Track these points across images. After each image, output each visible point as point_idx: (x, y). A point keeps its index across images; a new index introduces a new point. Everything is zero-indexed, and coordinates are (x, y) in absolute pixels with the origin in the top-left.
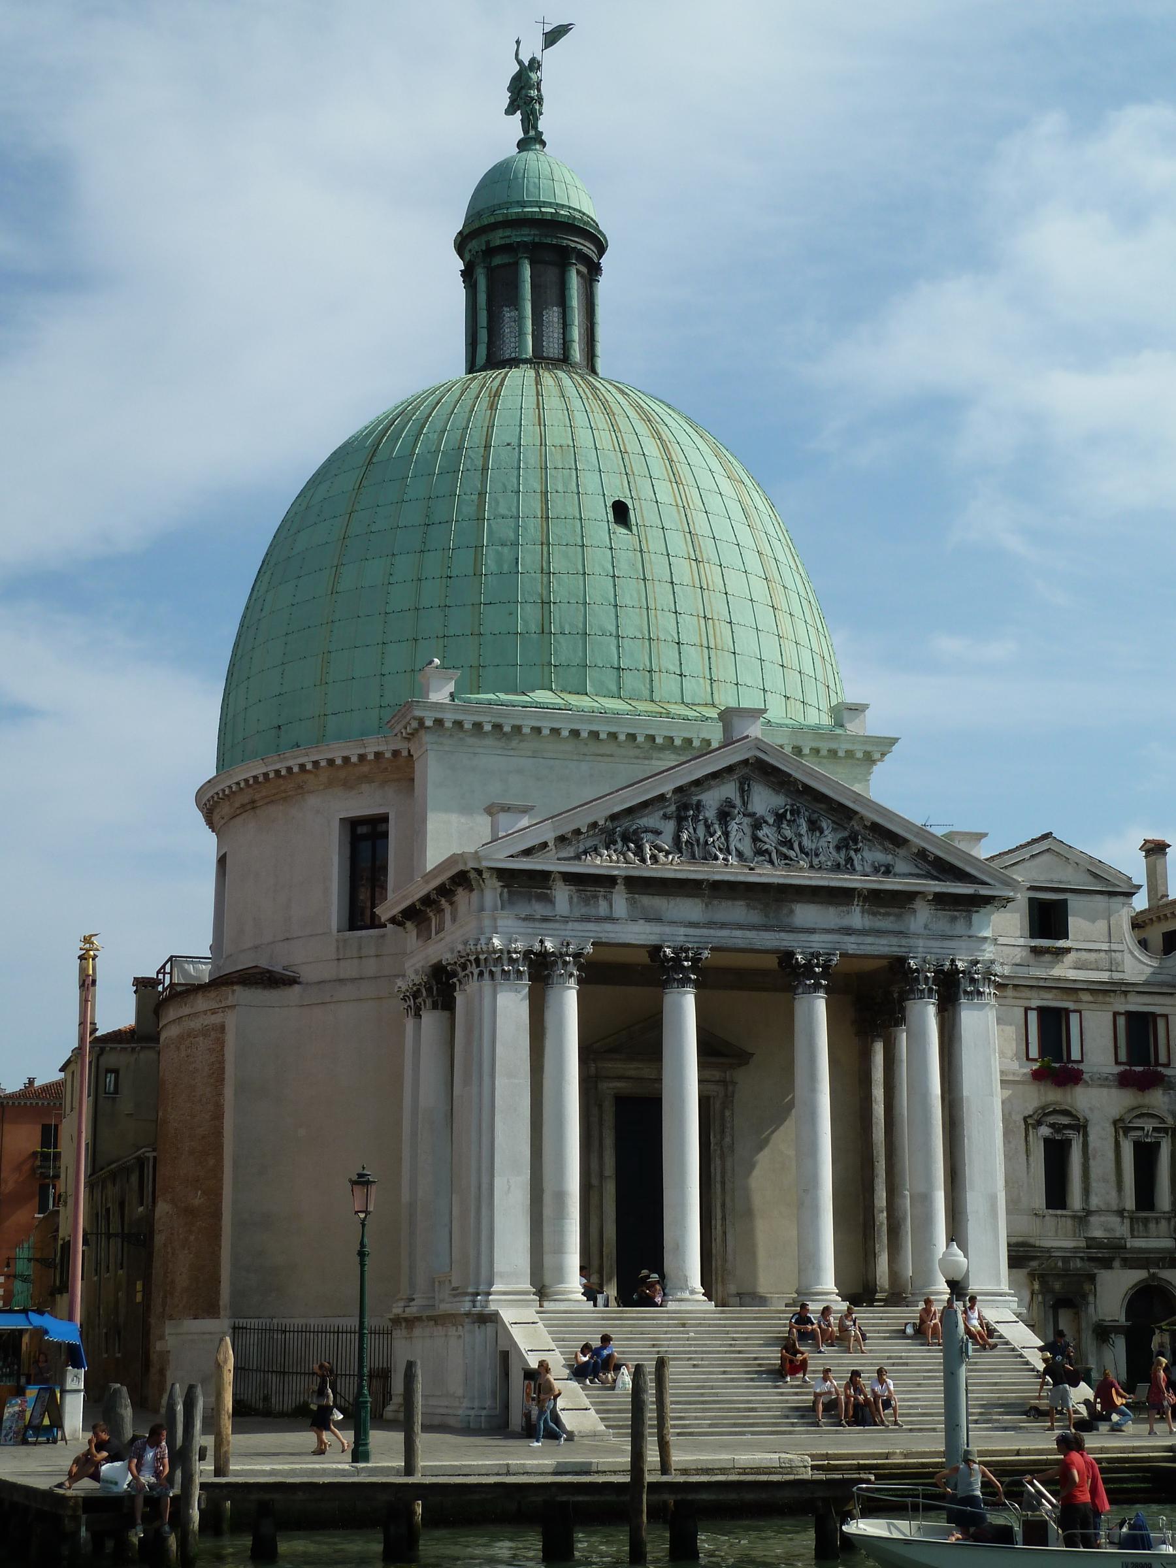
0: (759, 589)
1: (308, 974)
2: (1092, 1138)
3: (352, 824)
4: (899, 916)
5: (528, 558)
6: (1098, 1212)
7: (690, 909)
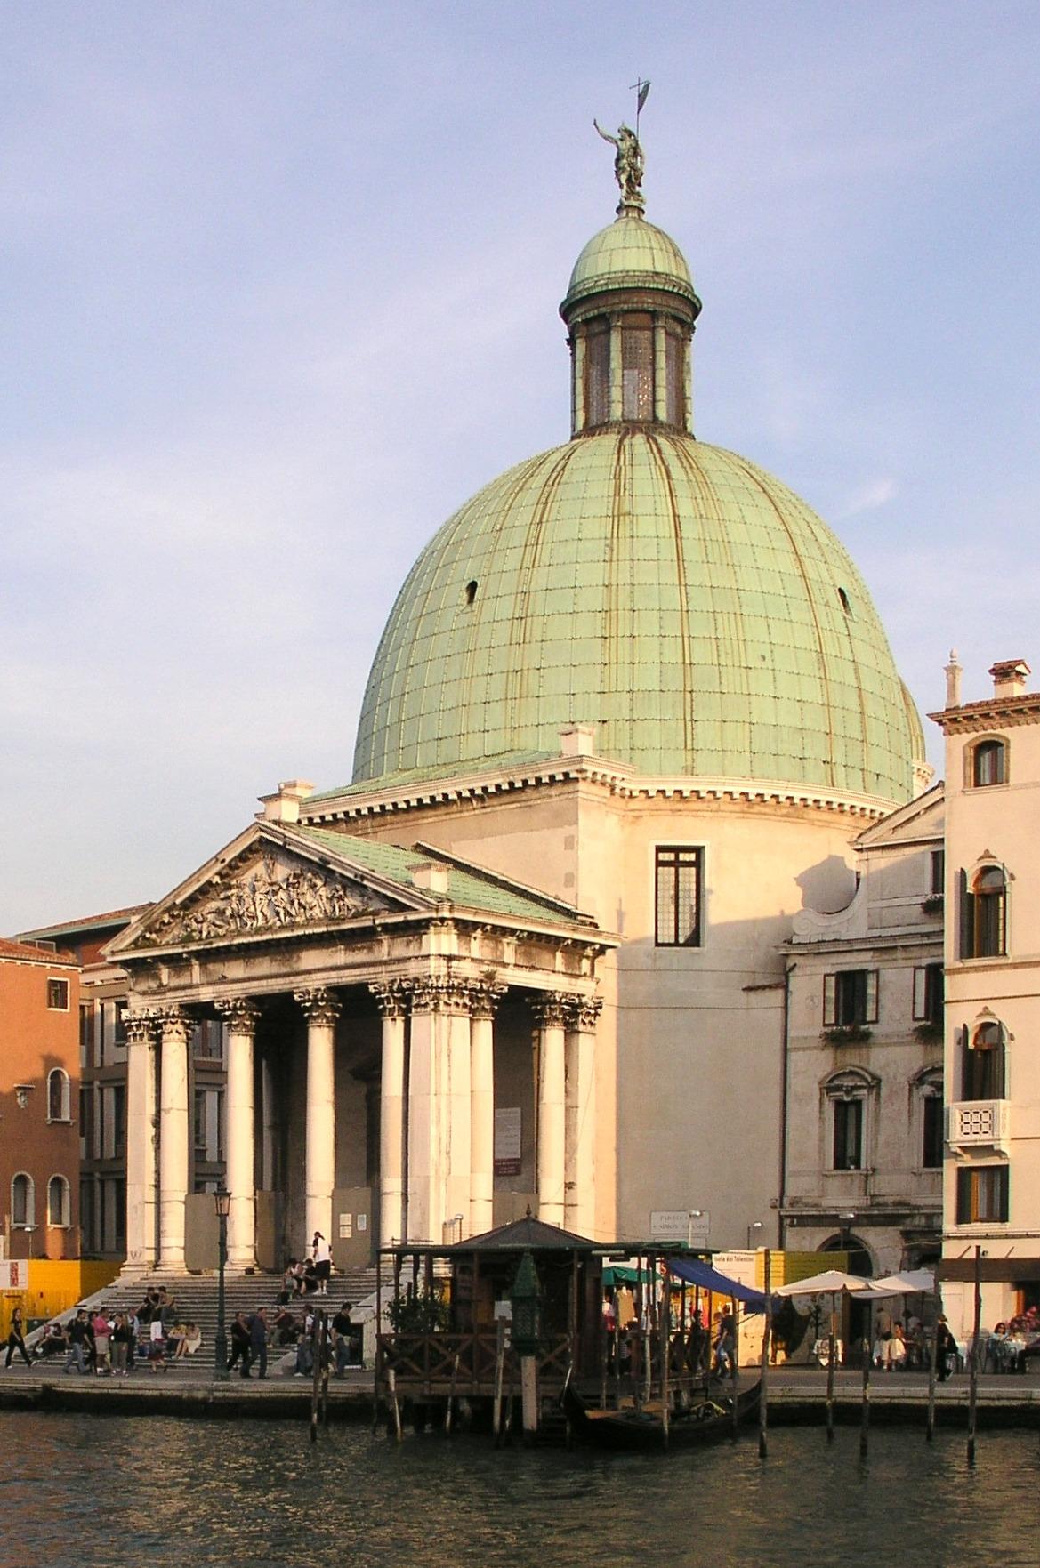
0: (589, 627)
4: (370, 949)
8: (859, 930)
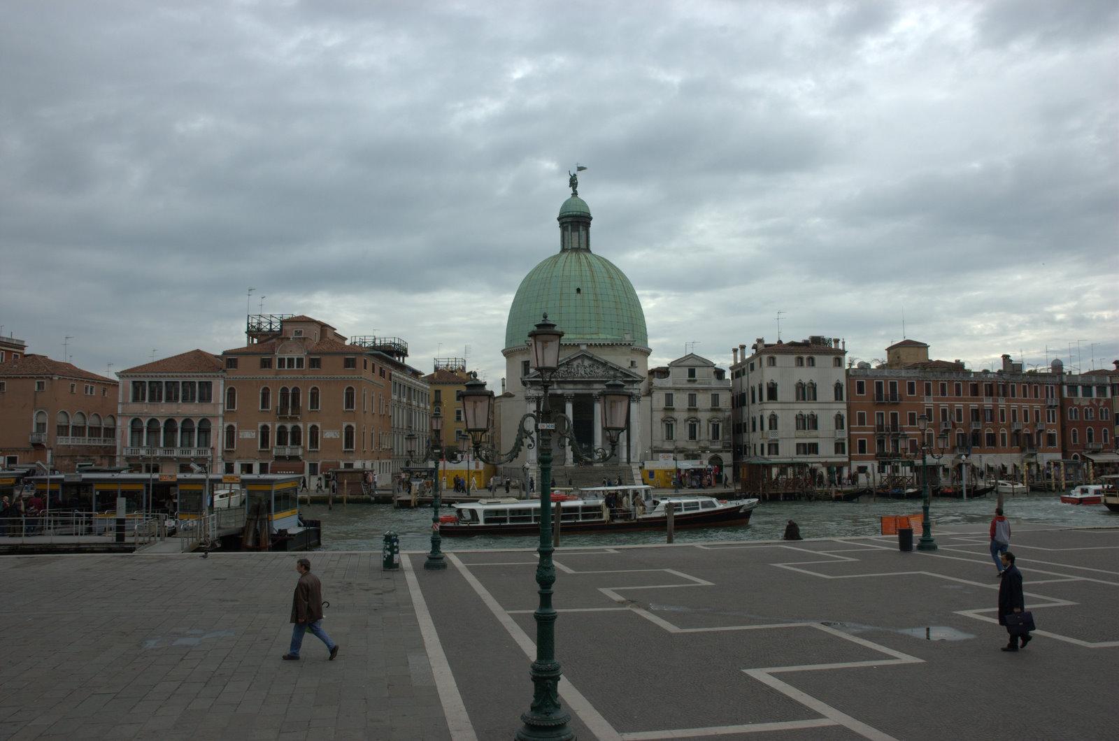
2: (702, 424)
6: (703, 440)
7: (571, 386)
8: (670, 385)
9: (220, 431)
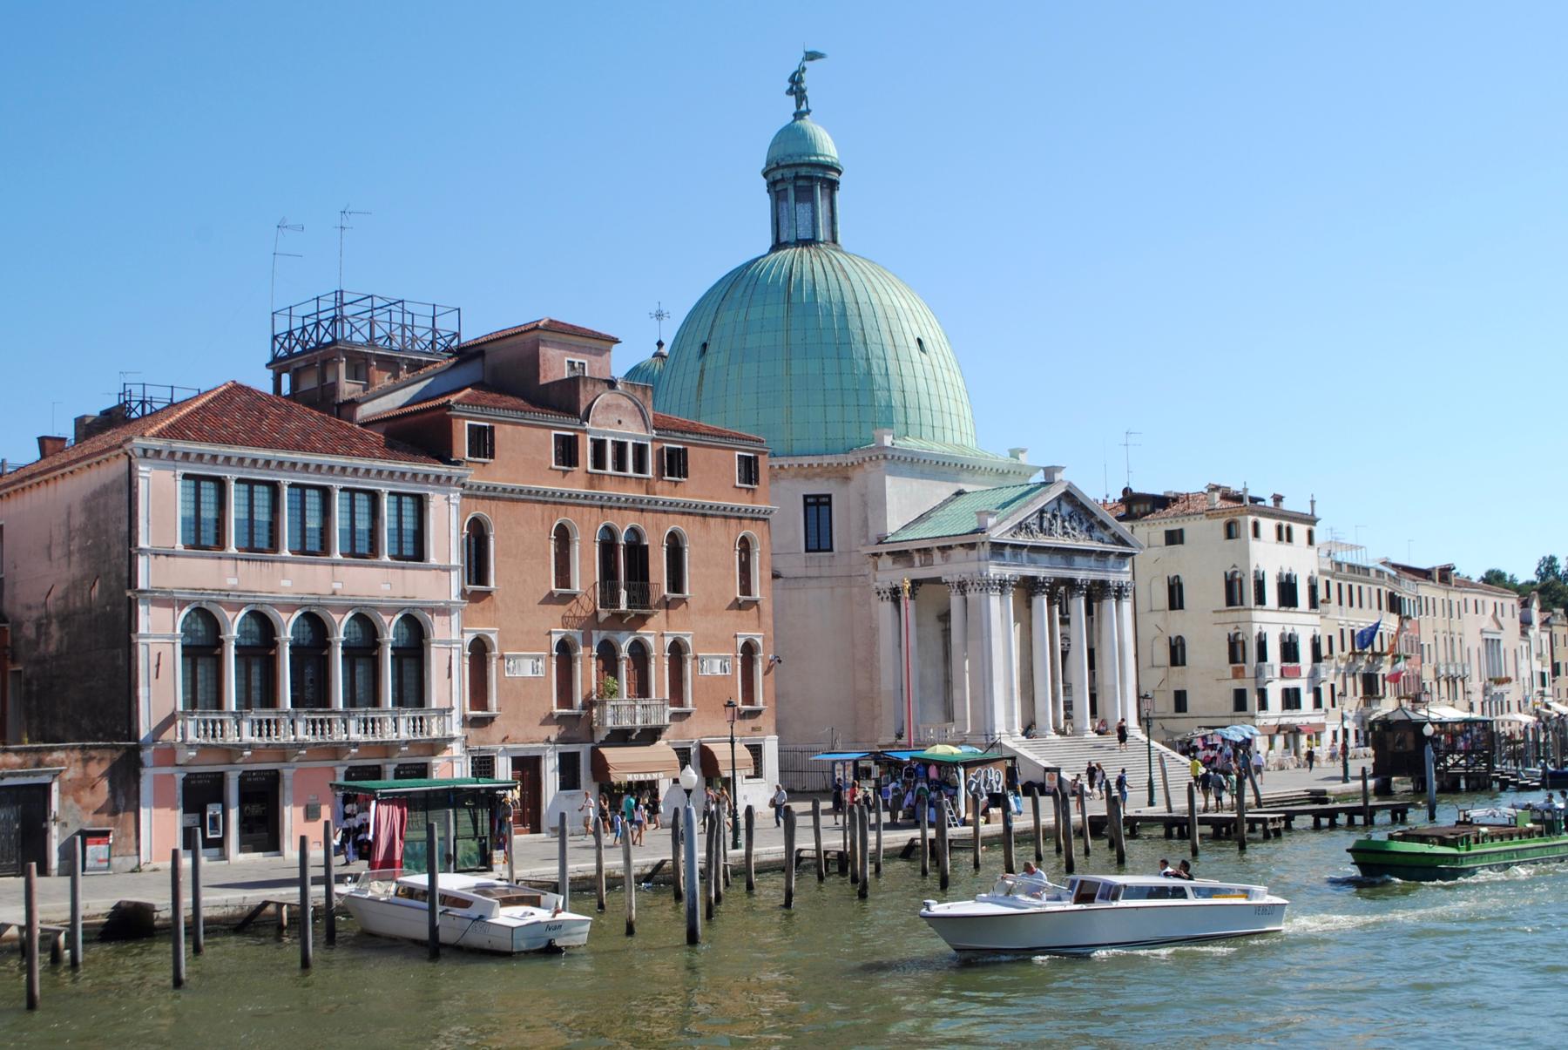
1: (784, 573)
3: (806, 497)
5: (892, 369)
7: (1044, 558)
9: (455, 654)
